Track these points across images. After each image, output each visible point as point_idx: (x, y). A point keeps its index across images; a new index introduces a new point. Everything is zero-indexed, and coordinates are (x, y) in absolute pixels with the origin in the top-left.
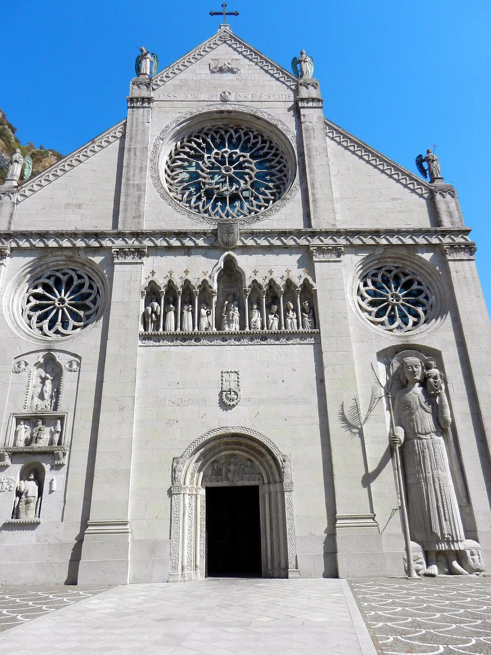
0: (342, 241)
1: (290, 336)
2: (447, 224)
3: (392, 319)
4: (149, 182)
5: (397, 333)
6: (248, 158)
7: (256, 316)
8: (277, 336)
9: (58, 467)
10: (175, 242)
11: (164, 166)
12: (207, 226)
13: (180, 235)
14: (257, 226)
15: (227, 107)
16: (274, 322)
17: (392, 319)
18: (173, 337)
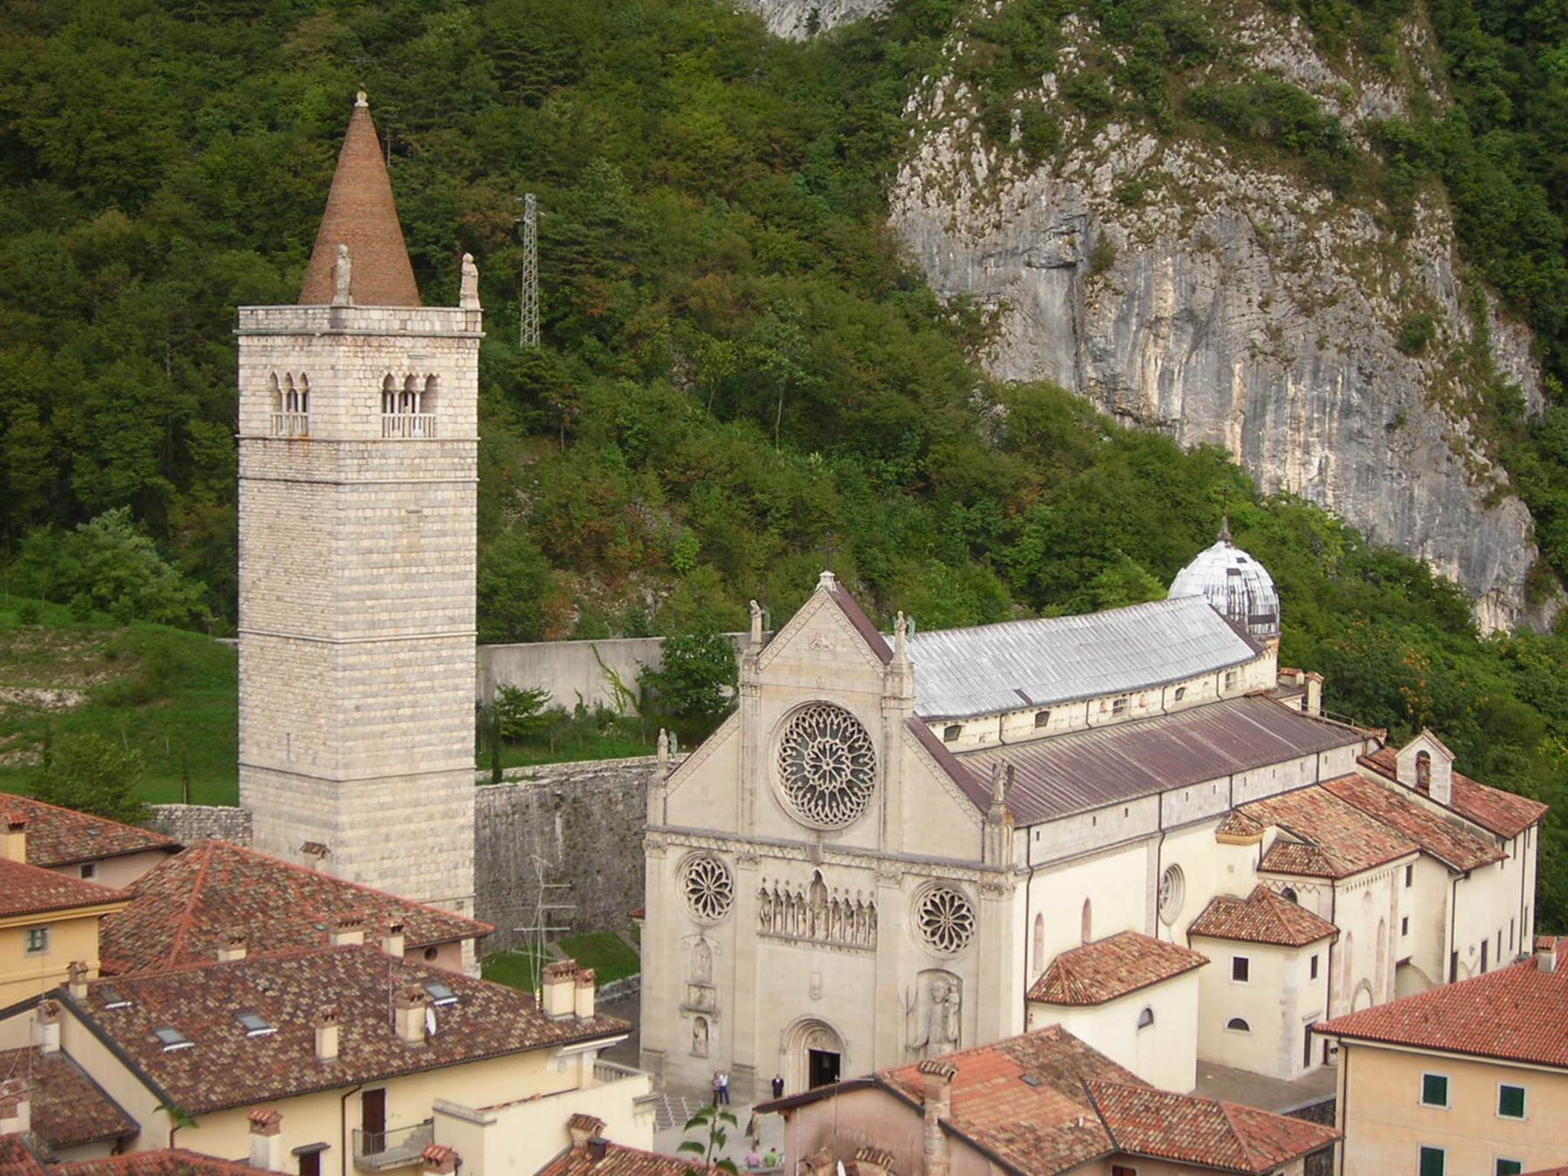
0: (901, 867)
1: (859, 948)
2: (988, 861)
3: (942, 939)
4: (761, 787)
5: (944, 954)
6: (846, 753)
7: (837, 926)
8: (849, 947)
9: (715, 1022)
10: (777, 851)
11: (777, 756)
12: (801, 836)
13: (782, 846)
14: (841, 841)
15: (823, 698)
16: (849, 931)
17: (942, 939)
18: (779, 937)
